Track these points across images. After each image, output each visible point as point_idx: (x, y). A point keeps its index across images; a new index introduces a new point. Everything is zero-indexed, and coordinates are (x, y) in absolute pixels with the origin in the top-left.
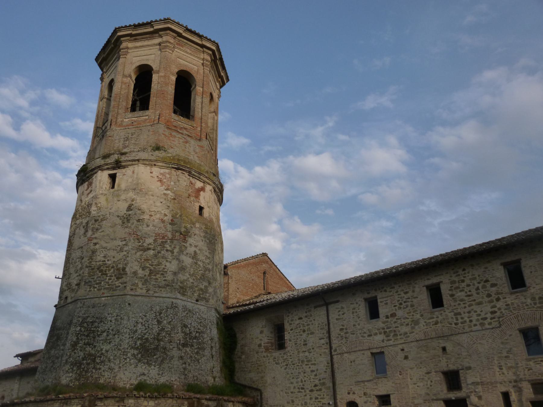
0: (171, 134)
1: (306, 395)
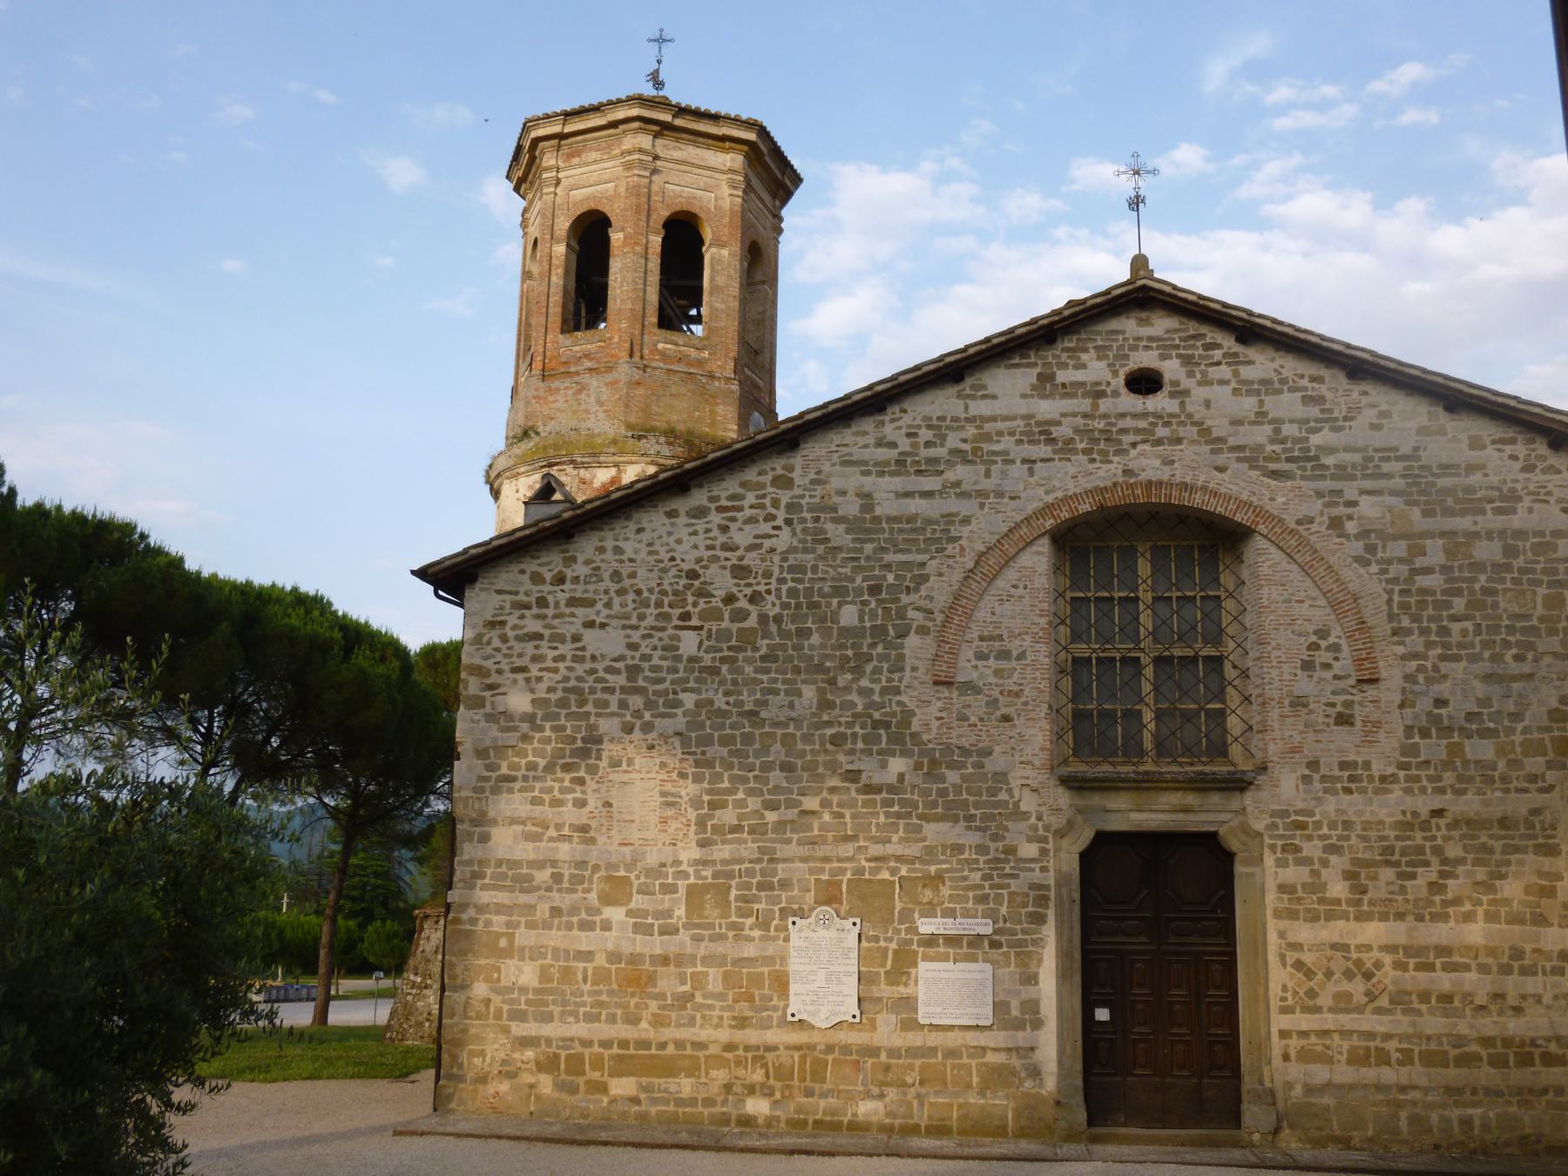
0: (550, 389)
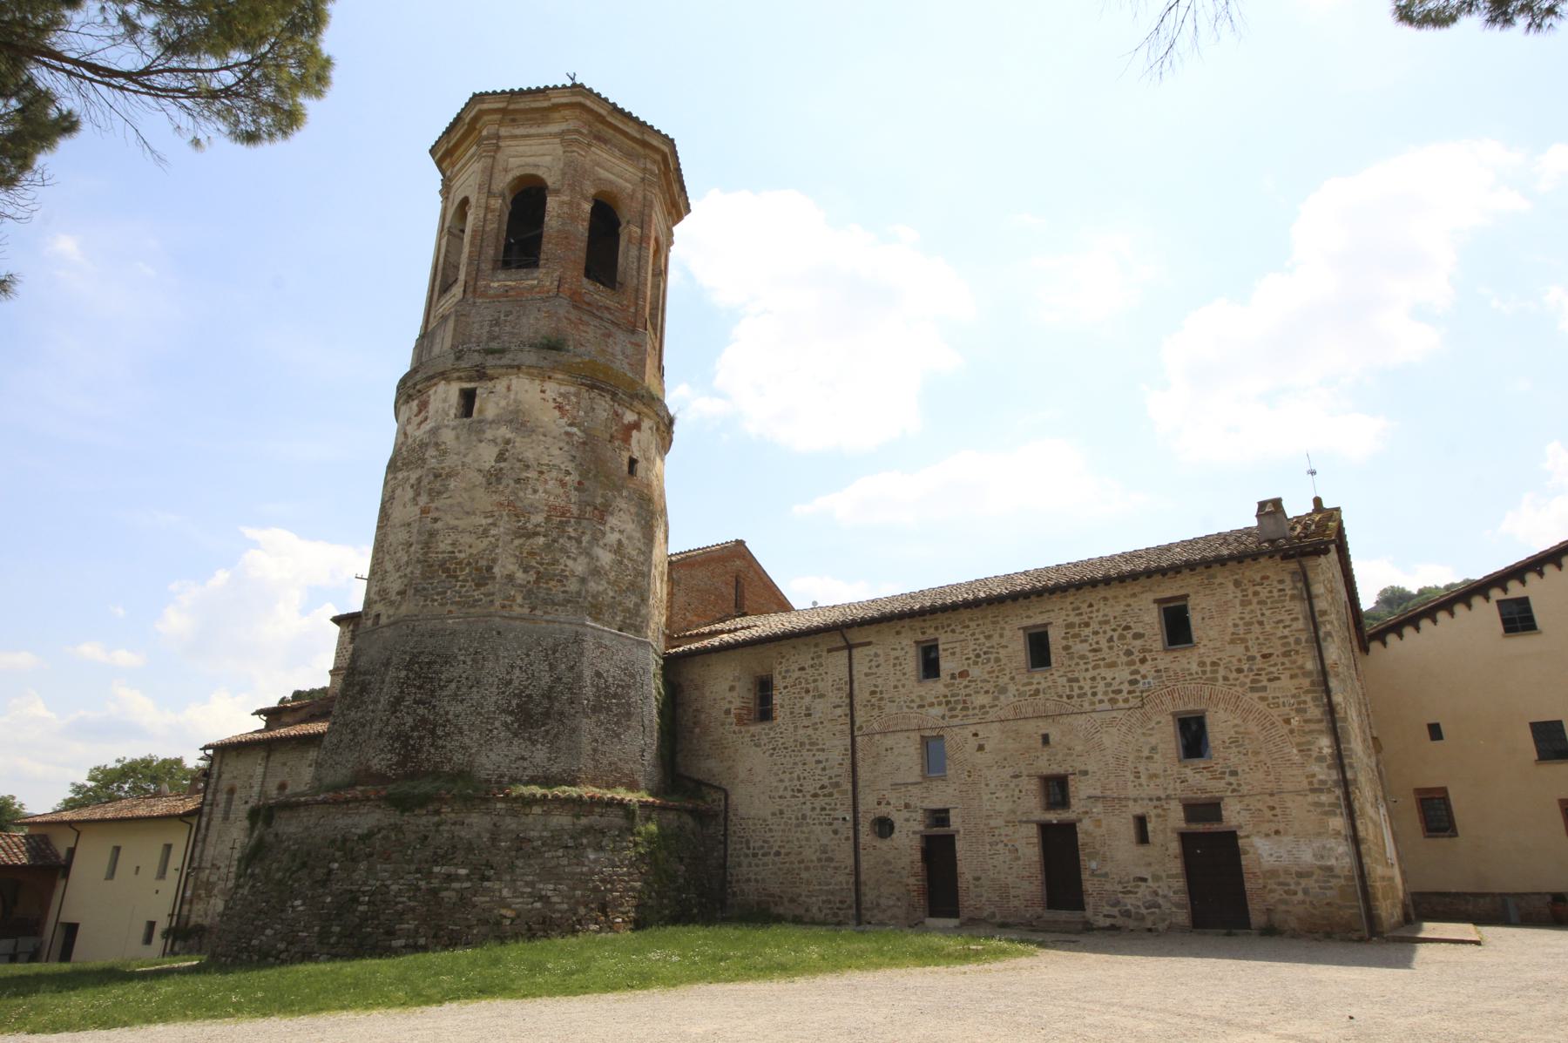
0: (580, 319)
1: (804, 803)
